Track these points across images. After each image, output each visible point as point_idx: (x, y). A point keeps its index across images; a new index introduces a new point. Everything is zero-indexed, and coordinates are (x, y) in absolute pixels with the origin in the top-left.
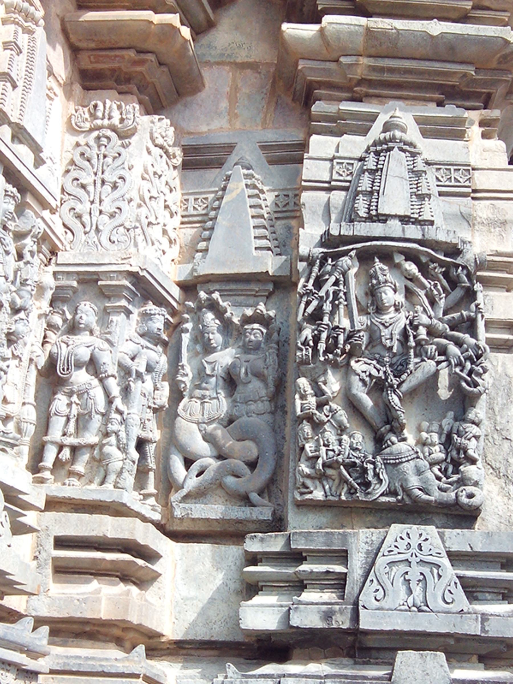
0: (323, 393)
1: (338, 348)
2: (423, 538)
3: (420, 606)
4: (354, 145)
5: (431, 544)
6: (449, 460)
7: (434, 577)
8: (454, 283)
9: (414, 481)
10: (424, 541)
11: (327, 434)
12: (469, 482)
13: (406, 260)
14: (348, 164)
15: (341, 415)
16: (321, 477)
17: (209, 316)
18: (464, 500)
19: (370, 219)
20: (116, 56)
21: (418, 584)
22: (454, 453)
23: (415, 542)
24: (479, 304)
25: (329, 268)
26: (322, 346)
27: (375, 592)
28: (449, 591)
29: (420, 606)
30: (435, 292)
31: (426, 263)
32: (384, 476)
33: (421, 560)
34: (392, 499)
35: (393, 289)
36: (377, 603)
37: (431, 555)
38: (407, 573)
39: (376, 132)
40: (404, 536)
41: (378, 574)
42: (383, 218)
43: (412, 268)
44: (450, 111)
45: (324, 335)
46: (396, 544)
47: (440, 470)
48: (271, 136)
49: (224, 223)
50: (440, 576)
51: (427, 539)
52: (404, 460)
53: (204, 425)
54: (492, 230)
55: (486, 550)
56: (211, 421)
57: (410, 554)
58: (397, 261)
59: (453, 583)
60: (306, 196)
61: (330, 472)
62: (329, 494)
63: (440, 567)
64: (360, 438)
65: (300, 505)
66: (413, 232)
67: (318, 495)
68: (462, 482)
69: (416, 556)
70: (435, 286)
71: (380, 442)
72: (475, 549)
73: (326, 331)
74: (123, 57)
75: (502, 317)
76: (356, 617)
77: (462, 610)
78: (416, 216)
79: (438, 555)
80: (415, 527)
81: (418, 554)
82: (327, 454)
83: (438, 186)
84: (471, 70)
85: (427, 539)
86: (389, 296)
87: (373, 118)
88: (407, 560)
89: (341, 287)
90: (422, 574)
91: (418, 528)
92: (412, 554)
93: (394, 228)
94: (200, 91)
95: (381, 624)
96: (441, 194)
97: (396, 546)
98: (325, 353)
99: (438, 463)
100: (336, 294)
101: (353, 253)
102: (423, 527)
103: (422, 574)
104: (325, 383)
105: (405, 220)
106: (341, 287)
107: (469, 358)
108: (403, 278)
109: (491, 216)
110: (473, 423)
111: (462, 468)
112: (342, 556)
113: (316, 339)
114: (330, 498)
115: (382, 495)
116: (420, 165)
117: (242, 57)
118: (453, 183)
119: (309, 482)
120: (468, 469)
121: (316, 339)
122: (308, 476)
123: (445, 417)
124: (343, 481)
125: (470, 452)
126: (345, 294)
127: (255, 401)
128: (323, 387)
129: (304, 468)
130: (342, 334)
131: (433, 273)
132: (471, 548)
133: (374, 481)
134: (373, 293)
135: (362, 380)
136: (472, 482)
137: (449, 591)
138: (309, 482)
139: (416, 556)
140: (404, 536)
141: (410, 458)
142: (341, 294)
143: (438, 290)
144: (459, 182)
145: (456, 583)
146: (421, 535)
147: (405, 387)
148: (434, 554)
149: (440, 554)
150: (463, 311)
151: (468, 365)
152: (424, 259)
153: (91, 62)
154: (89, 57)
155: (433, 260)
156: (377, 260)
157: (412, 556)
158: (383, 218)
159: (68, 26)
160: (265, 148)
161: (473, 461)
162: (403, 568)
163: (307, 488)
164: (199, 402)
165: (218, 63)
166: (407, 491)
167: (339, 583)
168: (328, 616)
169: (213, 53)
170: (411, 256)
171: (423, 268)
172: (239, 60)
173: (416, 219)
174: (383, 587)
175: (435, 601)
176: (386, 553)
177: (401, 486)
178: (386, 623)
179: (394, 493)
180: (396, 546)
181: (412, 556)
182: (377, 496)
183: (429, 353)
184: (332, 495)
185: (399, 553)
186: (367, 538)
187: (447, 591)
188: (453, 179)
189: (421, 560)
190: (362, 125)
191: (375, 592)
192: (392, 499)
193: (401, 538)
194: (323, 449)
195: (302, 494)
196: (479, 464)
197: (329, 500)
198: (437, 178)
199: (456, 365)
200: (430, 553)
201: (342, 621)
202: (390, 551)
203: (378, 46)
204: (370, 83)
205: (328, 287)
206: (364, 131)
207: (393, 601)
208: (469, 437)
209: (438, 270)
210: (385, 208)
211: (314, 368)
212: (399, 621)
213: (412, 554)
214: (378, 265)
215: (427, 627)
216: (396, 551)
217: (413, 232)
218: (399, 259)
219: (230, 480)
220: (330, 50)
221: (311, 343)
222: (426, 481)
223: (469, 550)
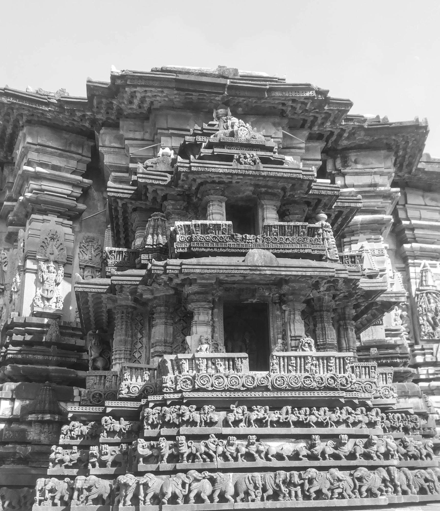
4: (418, 270)
16: (426, 335)
19: (426, 286)
39: (422, 266)
42: (428, 286)
43: (434, 295)
44: (434, 262)
48: (398, 265)
60: (411, 280)
64: (430, 328)
65: (421, 340)
66: (434, 288)
71: (434, 329)
76: (437, 359)
84: (438, 254)
86: (432, 301)
87: (420, 264)
93: (431, 288)
105: (433, 286)
112: (432, 349)
116: (433, 275)
124: (430, 336)
129: (423, 333)
134: (429, 300)
158: (428, 286)
160: (397, 268)
167: (432, 354)
168: (432, 359)
170: (434, 293)
171: (436, 295)
190: (419, 265)
201: (434, 360)
203: (422, 250)
204: (418, 256)
206: (419, 266)
210: (429, 284)
217: (434, 288)
220: (412, 250)
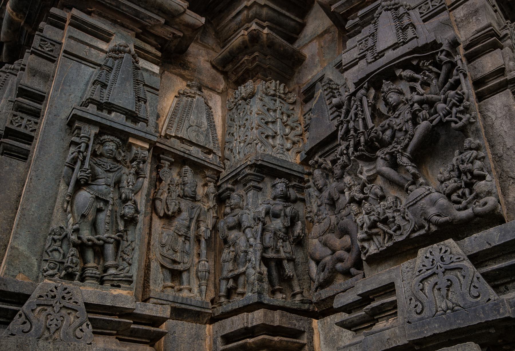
0: (361, 179)
1: (361, 146)
2: (443, 251)
3: (453, 308)
5: (451, 253)
6: (463, 186)
7: (459, 280)
8: (438, 65)
9: (432, 211)
10: (445, 252)
11: (367, 205)
12: (482, 195)
13: (404, 70)
14: (365, 41)
15: (375, 189)
17: (317, 172)
18: (479, 209)
20: (242, 64)
21: (448, 290)
22: (464, 178)
23: (437, 255)
24: (459, 67)
25: (352, 102)
26: (351, 150)
28: (474, 286)
29: (453, 308)
30: (426, 78)
31: (418, 64)
32: (410, 216)
33: (446, 270)
34: (422, 232)
35: (397, 92)
36: (419, 316)
37: (453, 262)
38: (436, 284)
40: (428, 255)
41: (415, 292)
42: (381, 54)
45: (352, 143)
46: (424, 264)
47: (458, 196)
49: (315, 116)
50: (464, 277)
51: (446, 251)
52: (419, 199)
53: (321, 237)
54: (471, 20)
55: (503, 242)
56: (324, 233)
57: (436, 267)
58: (398, 75)
59: (475, 279)
61: (374, 231)
62: (379, 247)
63: (462, 269)
67: (373, 249)
68: (478, 197)
69: (441, 268)
70: (424, 73)
72: (493, 245)
73: (352, 140)
74: (244, 62)
75: (492, 69)
77: (489, 300)
78: (402, 40)
79: (458, 260)
81: (442, 265)
82: (370, 219)
83: (421, 17)
85: (446, 251)
88: (434, 274)
89: (359, 108)
90: (448, 280)
91: (438, 246)
92: (437, 267)
94: (304, 60)
95: (423, 332)
96: (424, 21)
97: (424, 266)
98: (353, 153)
99: (455, 190)
100: (356, 115)
101: (366, 85)
102: (442, 243)
103: (448, 280)
104: (361, 173)
105: (394, 47)
106: (359, 108)
107: (454, 105)
108: (407, 83)
109: (465, 13)
110: (471, 149)
111: (475, 187)
113: (347, 148)
114: (381, 249)
115: (413, 231)
117: (320, 30)
118: (431, 9)
119: (366, 245)
120: (481, 186)
121: (347, 148)
122: (363, 240)
123: (454, 156)
124: (385, 233)
125: (476, 172)
126: (362, 111)
127: (344, 208)
128: (360, 176)
130: (362, 136)
131: (425, 68)
132: (490, 244)
133: (402, 223)
135: (382, 158)
136: (485, 193)
137: (474, 286)
138: (366, 245)
139: (441, 268)
140: (428, 255)
141: (423, 196)
142: (360, 112)
143: (428, 76)
144: (436, 5)
145: (478, 278)
146: (441, 249)
147: (409, 149)
148: (455, 260)
149: (459, 258)
150: (450, 80)
151: (454, 110)
152: (415, 63)
153: (235, 75)
154: (232, 73)
155: (420, 59)
156: (384, 81)
158: (381, 54)
159: (213, 63)
161: (482, 178)
162: (432, 280)
163: (365, 248)
164: (317, 224)
165: (310, 42)
166: (429, 221)
169: (307, 38)
170: (405, 65)
172: (320, 33)
173: (403, 42)
174: (420, 302)
175: (464, 299)
176: (417, 274)
177: (425, 219)
178: (426, 330)
179: (422, 227)
180: (424, 266)
181: (437, 269)
182: (408, 233)
183: (422, 117)
184: (381, 247)
185: (427, 270)
186: (407, 268)
187: (472, 288)
188: (431, 7)
189: (446, 270)
192: (422, 232)
193: (426, 257)
194: (366, 216)
195: (365, 254)
196: (488, 177)
197: (381, 251)
198: (421, 13)
199: (445, 116)
200: (451, 261)
202: (419, 271)
205: (352, 112)
207: (430, 310)
208: (470, 160)
209: (427, 64)
211: (351, 167)
212: (436, 325)
213: (437, 267)
214: (387, 85)
215: (460, 324)
216: (424, 269)
218: (398, 73)
219: (339, 265)
221: (345, 152)
222: (442, 207)
223: (488, 247)
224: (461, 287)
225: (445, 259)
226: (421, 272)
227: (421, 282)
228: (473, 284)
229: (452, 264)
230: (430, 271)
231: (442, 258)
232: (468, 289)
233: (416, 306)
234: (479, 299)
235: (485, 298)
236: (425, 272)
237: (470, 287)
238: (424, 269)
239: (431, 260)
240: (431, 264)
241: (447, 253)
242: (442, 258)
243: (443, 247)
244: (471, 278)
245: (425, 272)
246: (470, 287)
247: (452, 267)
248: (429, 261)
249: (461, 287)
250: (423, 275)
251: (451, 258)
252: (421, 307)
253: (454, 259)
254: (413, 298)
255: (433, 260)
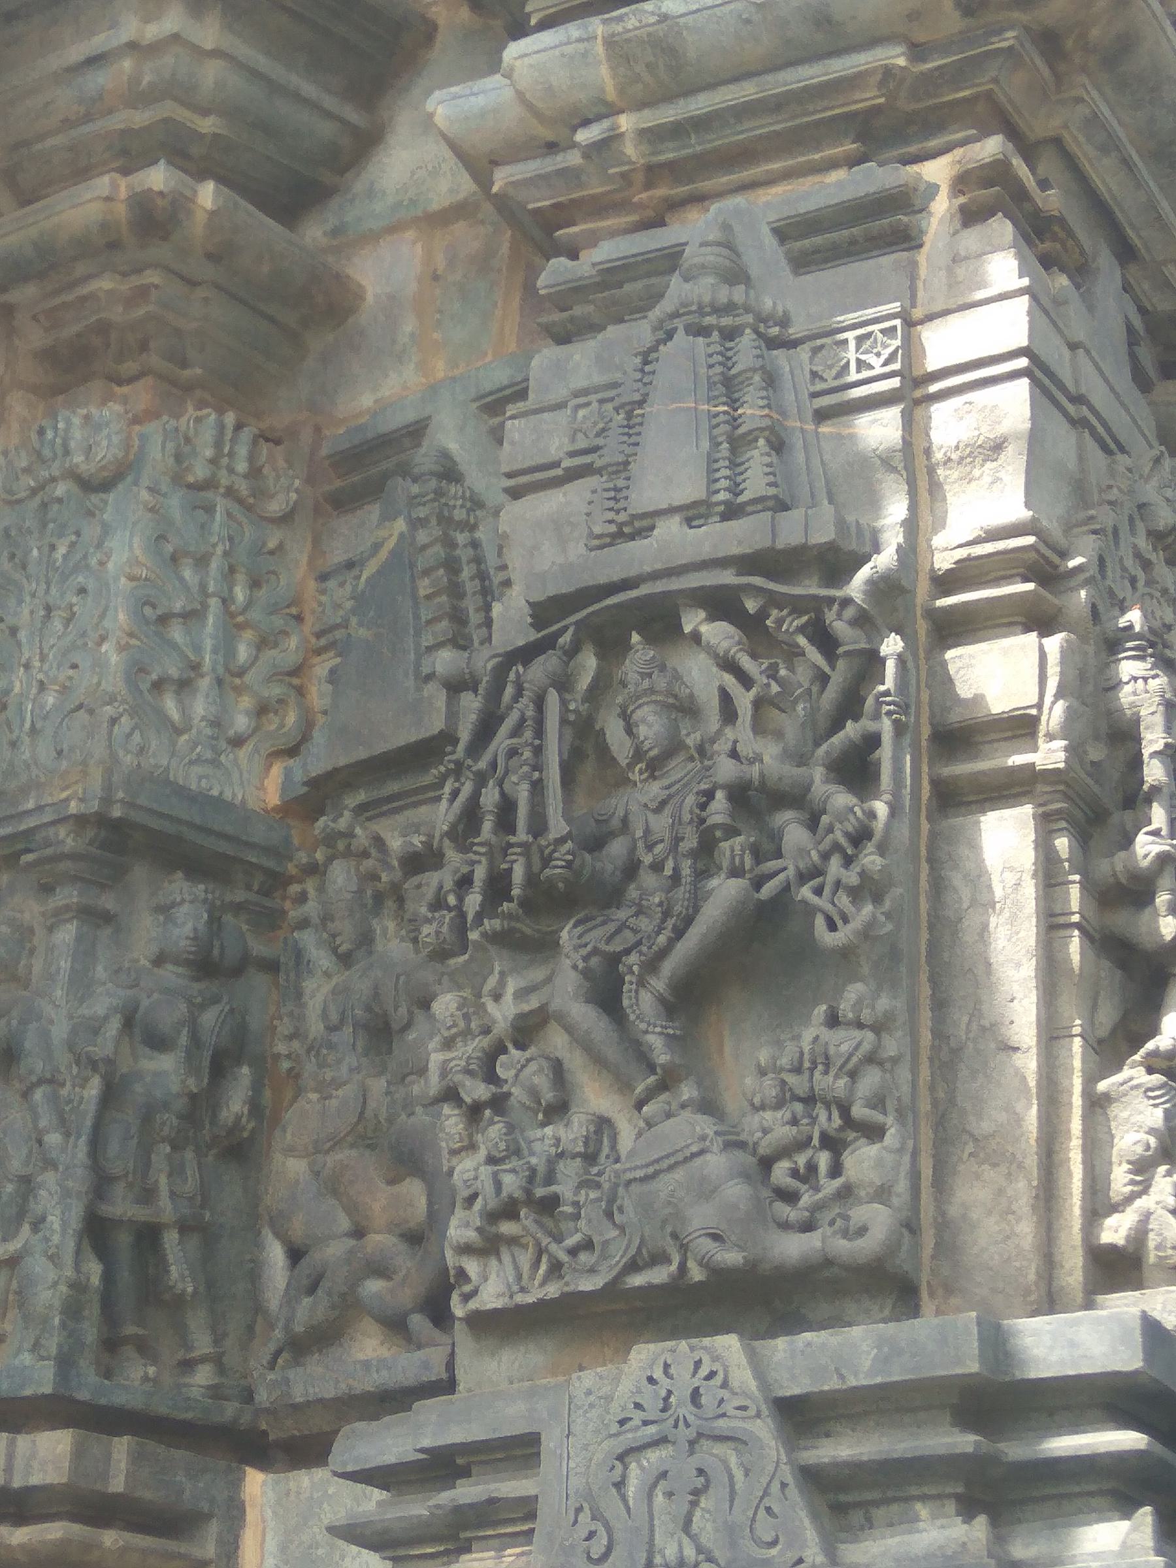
23: (684, 1381)
27: (587, 1539)
28: (768, 1510)
33: (700, 1435)
37: (724, 1415)
38: (664, 1475)
40: (658, 1374)
57: (671, 1421)
59: (775, 1487)
69: (687, 1425)
77: (800, 1561)
80: (683, 1345)
85: (712, 1375)
97: (638, 1406)
103: (701, 1472)
137: (768, 1510)
139: (687, 1425)
140: (658, 1374)
145: (784, 1485)
146: (698, 1364)
157: (676, 1426)
175: (733, 1545)
176: (615, 1428)
180: (638, 1406)
181: (676, 1426)
185: (646, 1423)
187: (762, 1512)
191: (587, 1539)
193: (651, 1380)
202: (622, 1422)
216: (638, 1416)
224: (732, 1501)
225: (703, 1400)
226: (627, 1426)
227: (621, 1458)
228: (767, 1502)
229: (721, 1423)
230: (652, 1430)
231: (696, 1394)
232: (750, 1514)
233: (591, 1535)
234: (774, 1552)
235: (789, 1554)
236: (637, 1428)
237: (757, 1507)
238: (638, 1416)
239: (663, 1393)
240: (661, 1406)
241: (712, 1382)
242: (696, 1394)
243: (706, 1360)
244: (764, 1481)
245: (637, 1428)
246: (757, 1507)
247: (717, 1433)
248: (656, 1393)
249: (732, 1501)
250: (630, 1435)
251: (722, 1401)
252: (605, 1542)
253: (729, 1408)
254: (586, 1505)
255: (670, 1393)
